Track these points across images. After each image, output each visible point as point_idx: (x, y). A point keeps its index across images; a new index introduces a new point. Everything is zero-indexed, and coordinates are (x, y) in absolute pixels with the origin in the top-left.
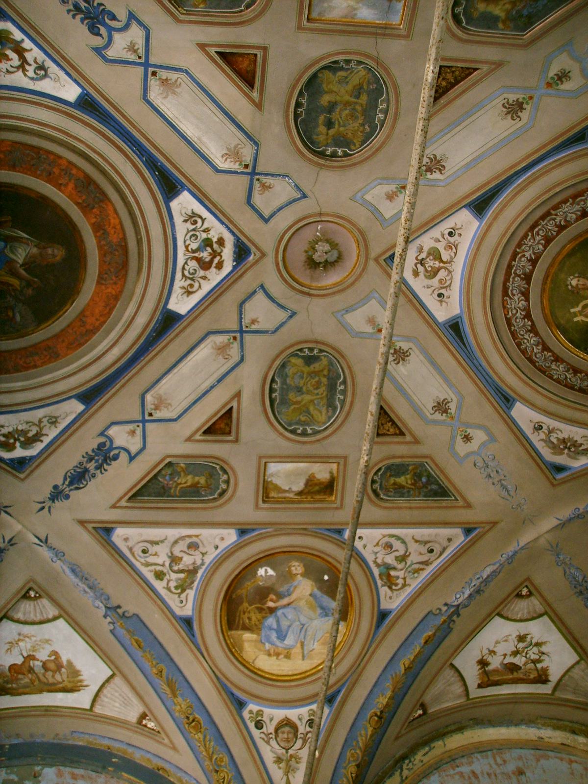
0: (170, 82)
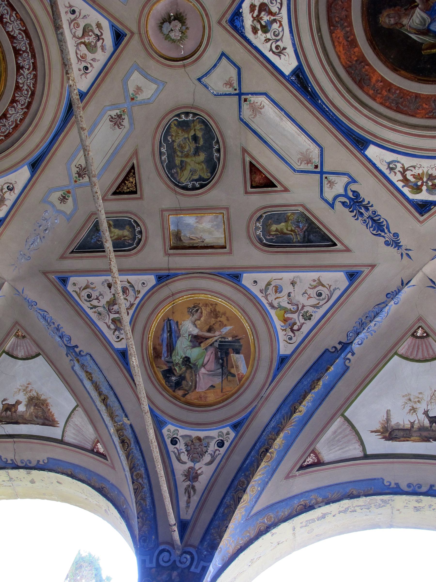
0: (306, 162)
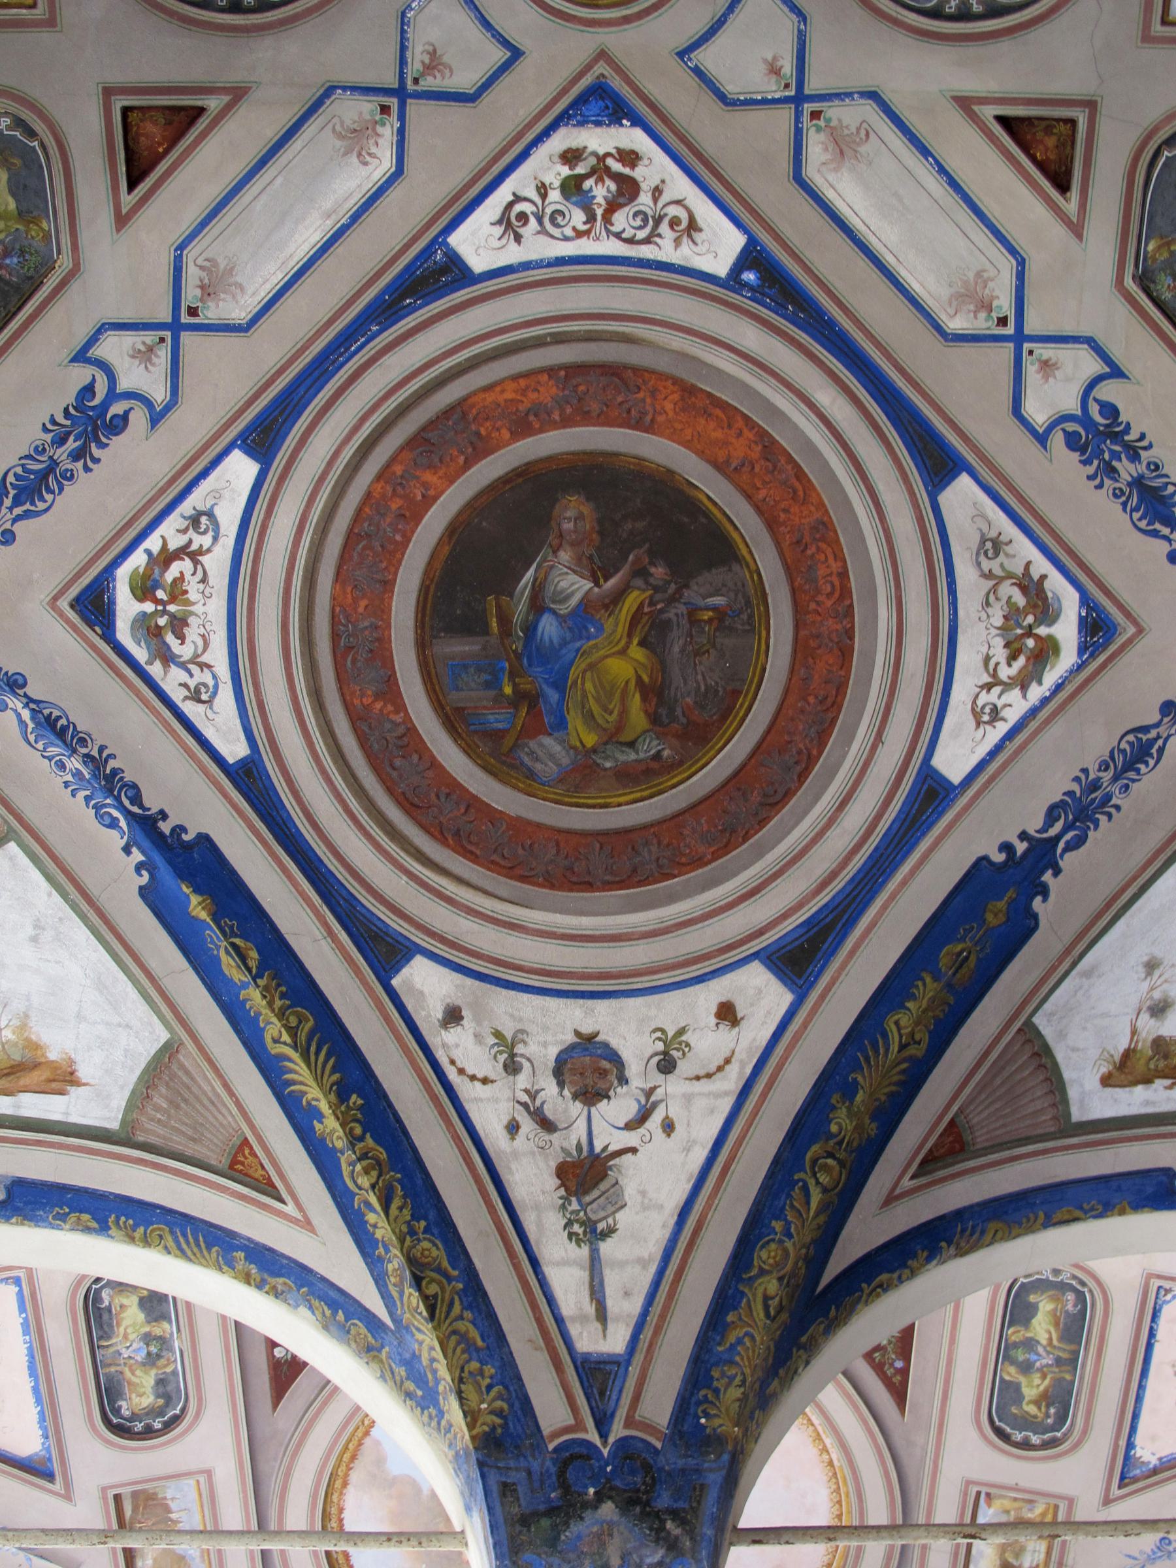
0: (206, 281)
